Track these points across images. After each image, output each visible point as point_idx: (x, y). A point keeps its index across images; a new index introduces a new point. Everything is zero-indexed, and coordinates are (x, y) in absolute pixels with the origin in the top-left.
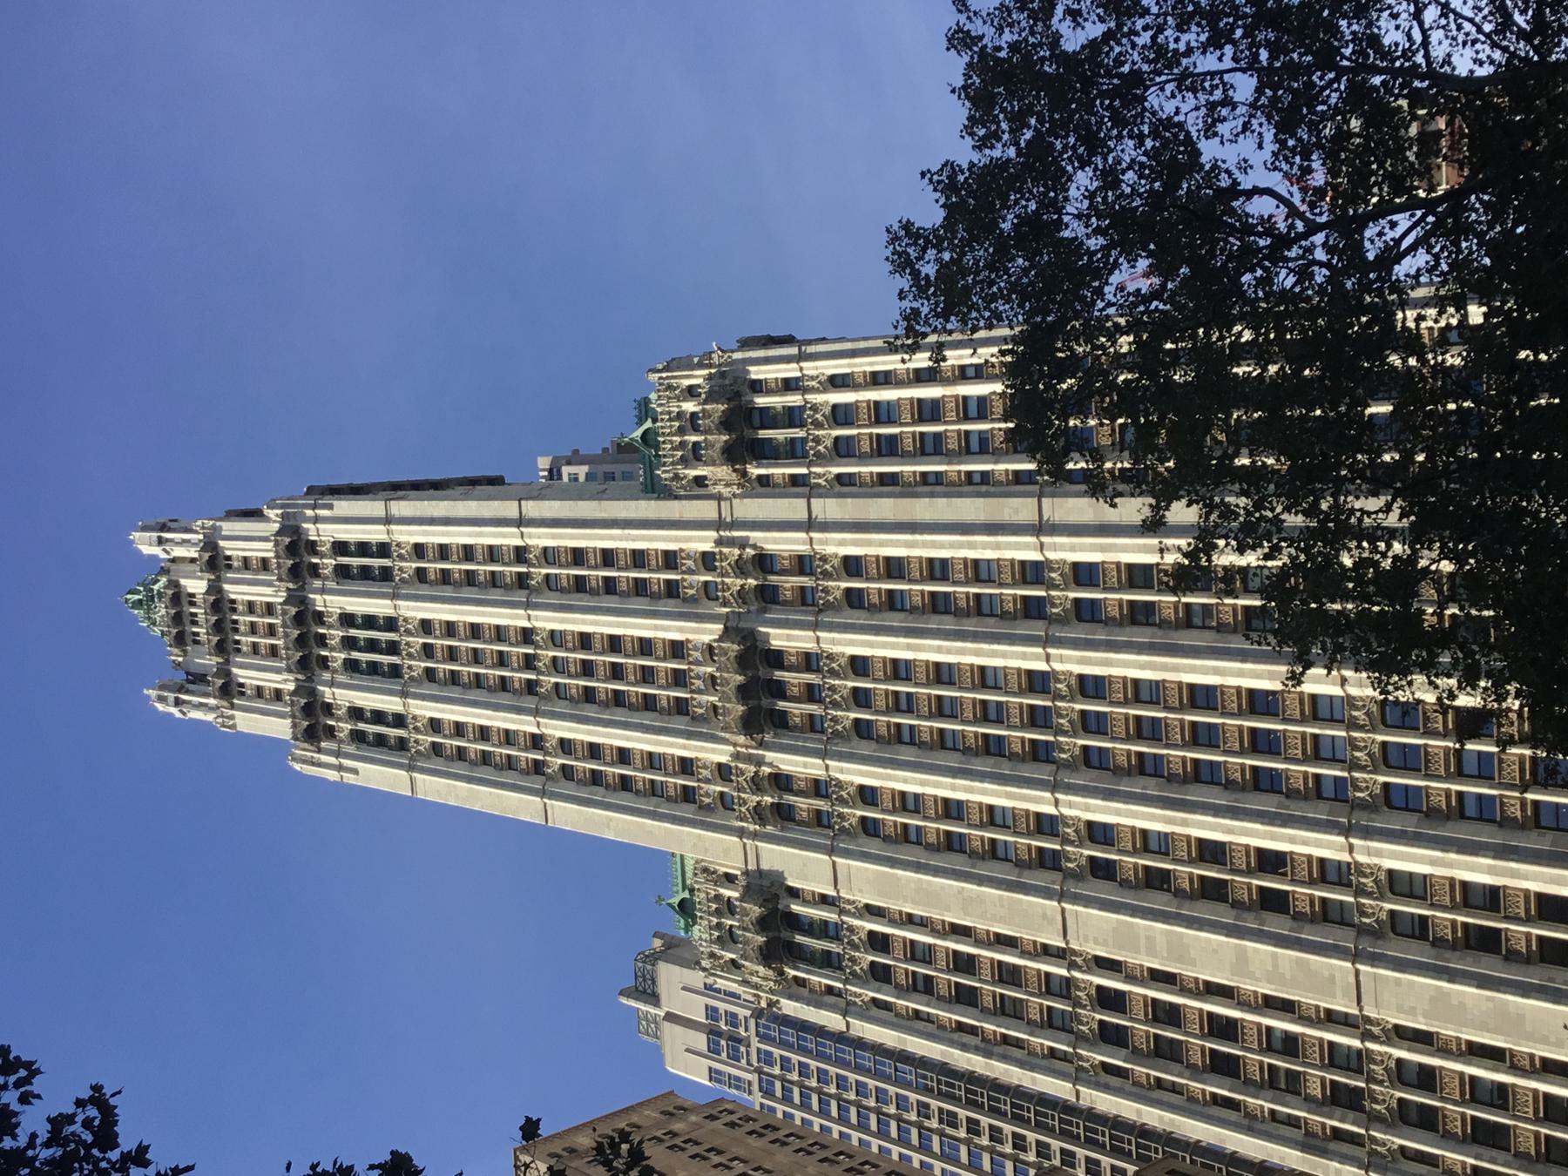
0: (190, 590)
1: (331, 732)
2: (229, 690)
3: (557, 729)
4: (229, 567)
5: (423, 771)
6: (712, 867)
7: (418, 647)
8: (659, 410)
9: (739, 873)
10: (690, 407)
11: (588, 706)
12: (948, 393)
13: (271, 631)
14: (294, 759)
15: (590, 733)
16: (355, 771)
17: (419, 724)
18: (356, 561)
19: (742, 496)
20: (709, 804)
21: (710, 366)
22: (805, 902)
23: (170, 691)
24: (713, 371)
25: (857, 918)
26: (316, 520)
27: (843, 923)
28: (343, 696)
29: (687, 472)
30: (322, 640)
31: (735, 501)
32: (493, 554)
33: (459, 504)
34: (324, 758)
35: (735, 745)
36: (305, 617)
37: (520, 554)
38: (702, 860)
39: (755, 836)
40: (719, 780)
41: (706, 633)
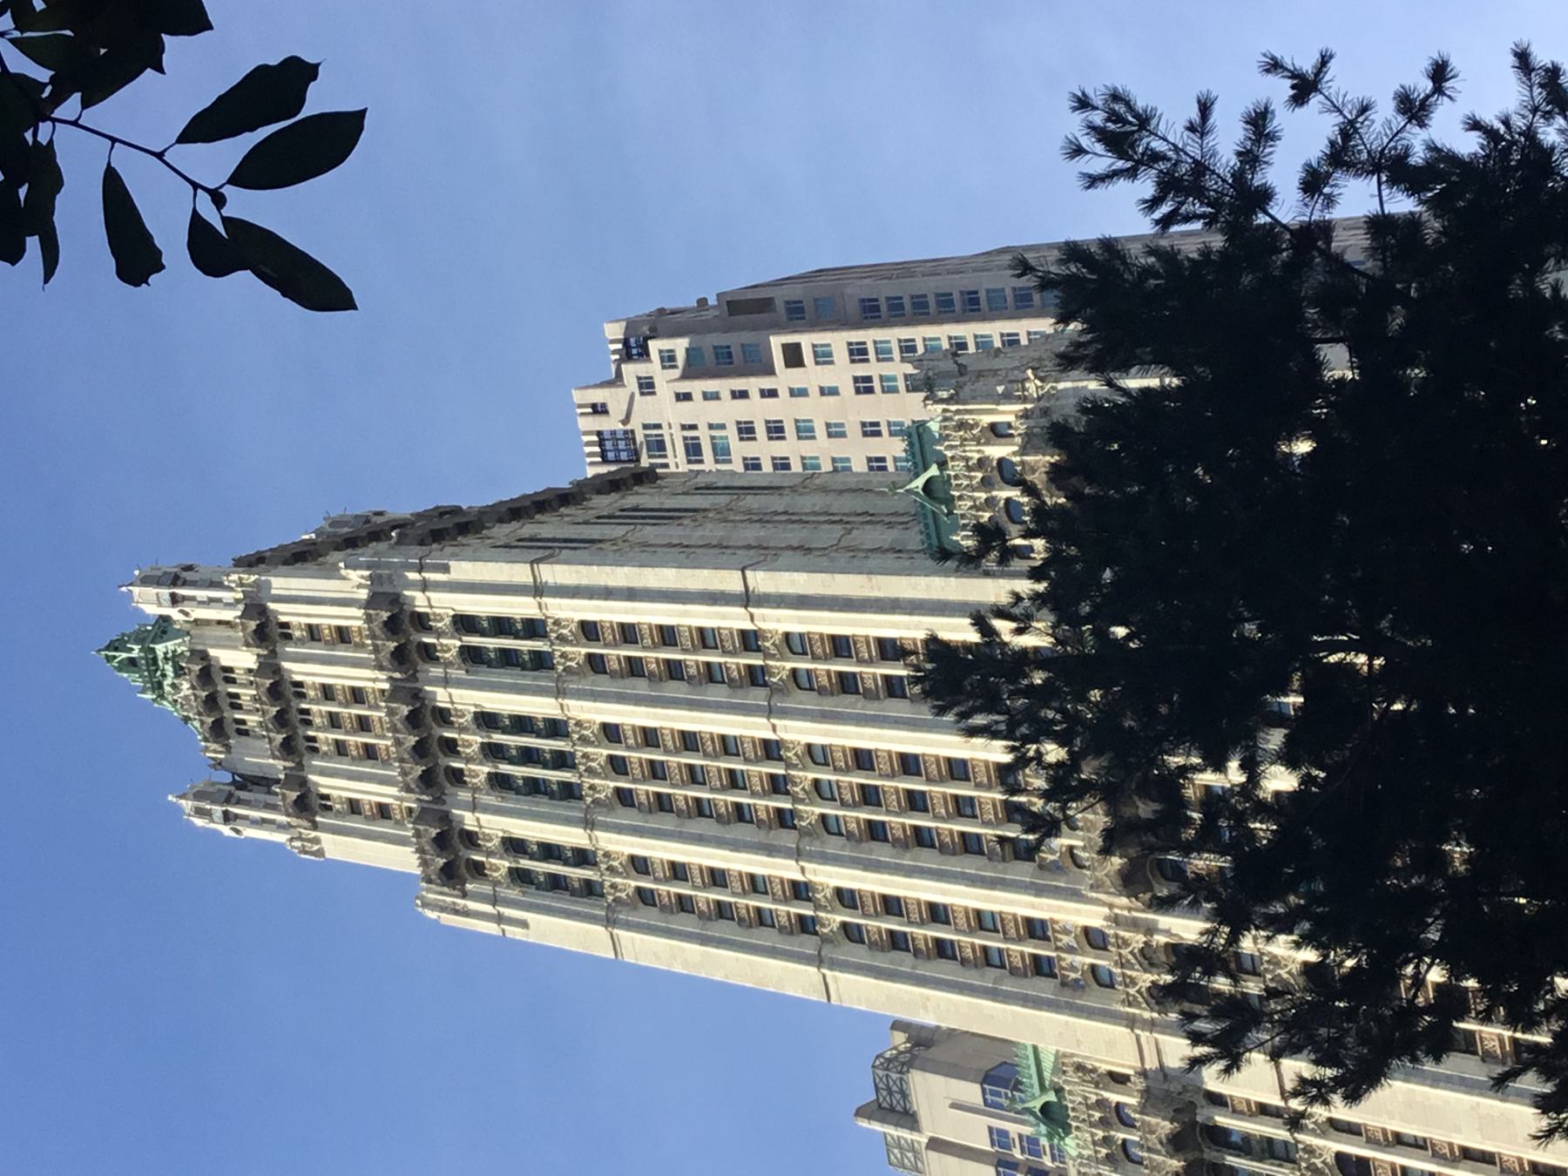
0: (225, 663)
1: (478, 870)
2: (308, 805)
3: (828, 877)
4: (288, 637)
5: (628, 926)
6: (1089, 1064)
7: (602, 760)
8: (949, 454)
9: (1131, 1072)
10: (996, 451)
11: (875, 845)
13: (363, 725)
14: (425, 905)
15: (883, 883)
16: (524, 924)
17: (615, 864)
18: (492, 643)
20: (1076, 980)
21: (1024, 399)
22: (1236, 1113)
23: (213, 802)
24: (1029, 406)
25: (1317, 1136)
26: (425, 586)
27: (1297, 1142)
30: (451, 747)
32: (705, 639)
33: (648, 571)
34: (472, 905)
35: (1111, 906)
37: (750, 641)
38: (1072, 1055)
39: (1152, 1025)
40: (1088, 948)
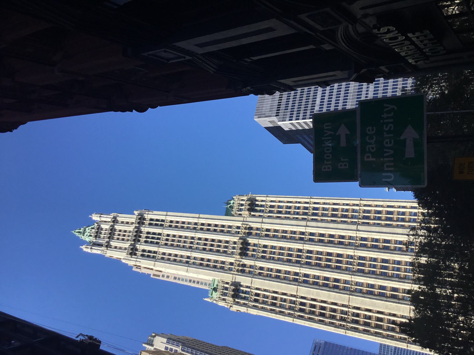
12: (293, 205)
19: (249, 217)
29: (238, 212)
31: (247, 218)
41: (236, 239)
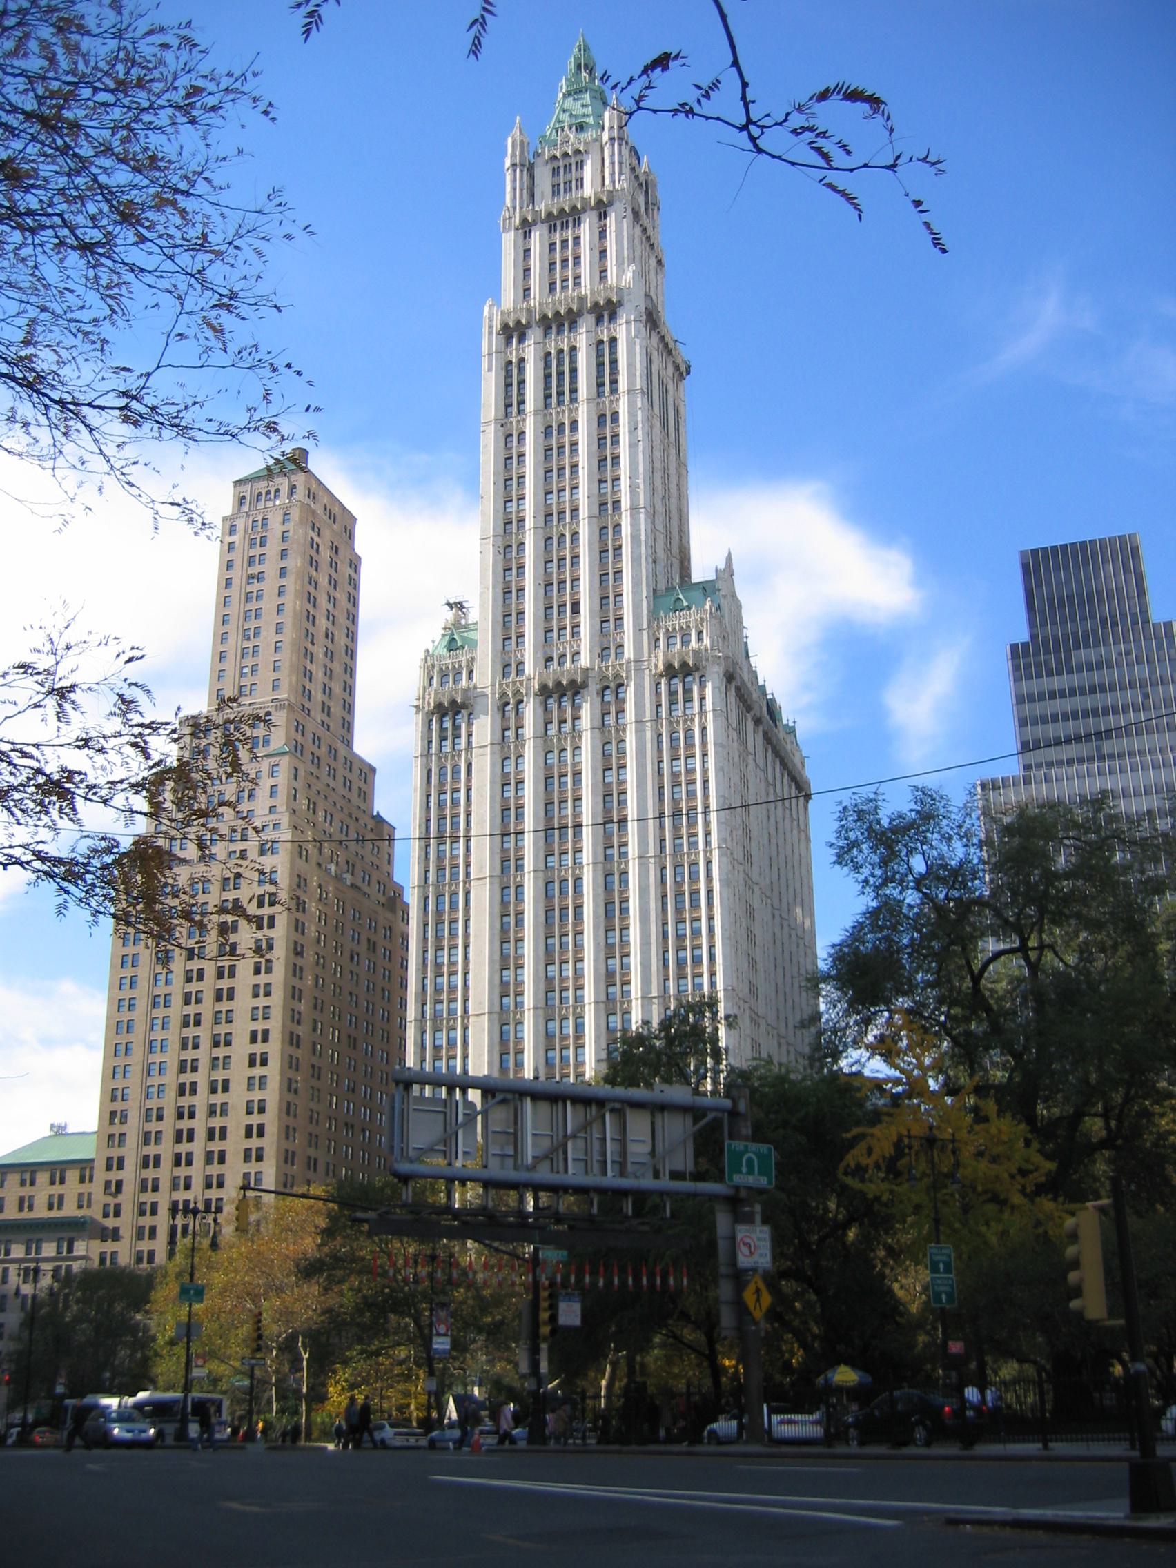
2: (526, 227)
26: (628, 322)
28: (530, 351)
36: (569, 319)
